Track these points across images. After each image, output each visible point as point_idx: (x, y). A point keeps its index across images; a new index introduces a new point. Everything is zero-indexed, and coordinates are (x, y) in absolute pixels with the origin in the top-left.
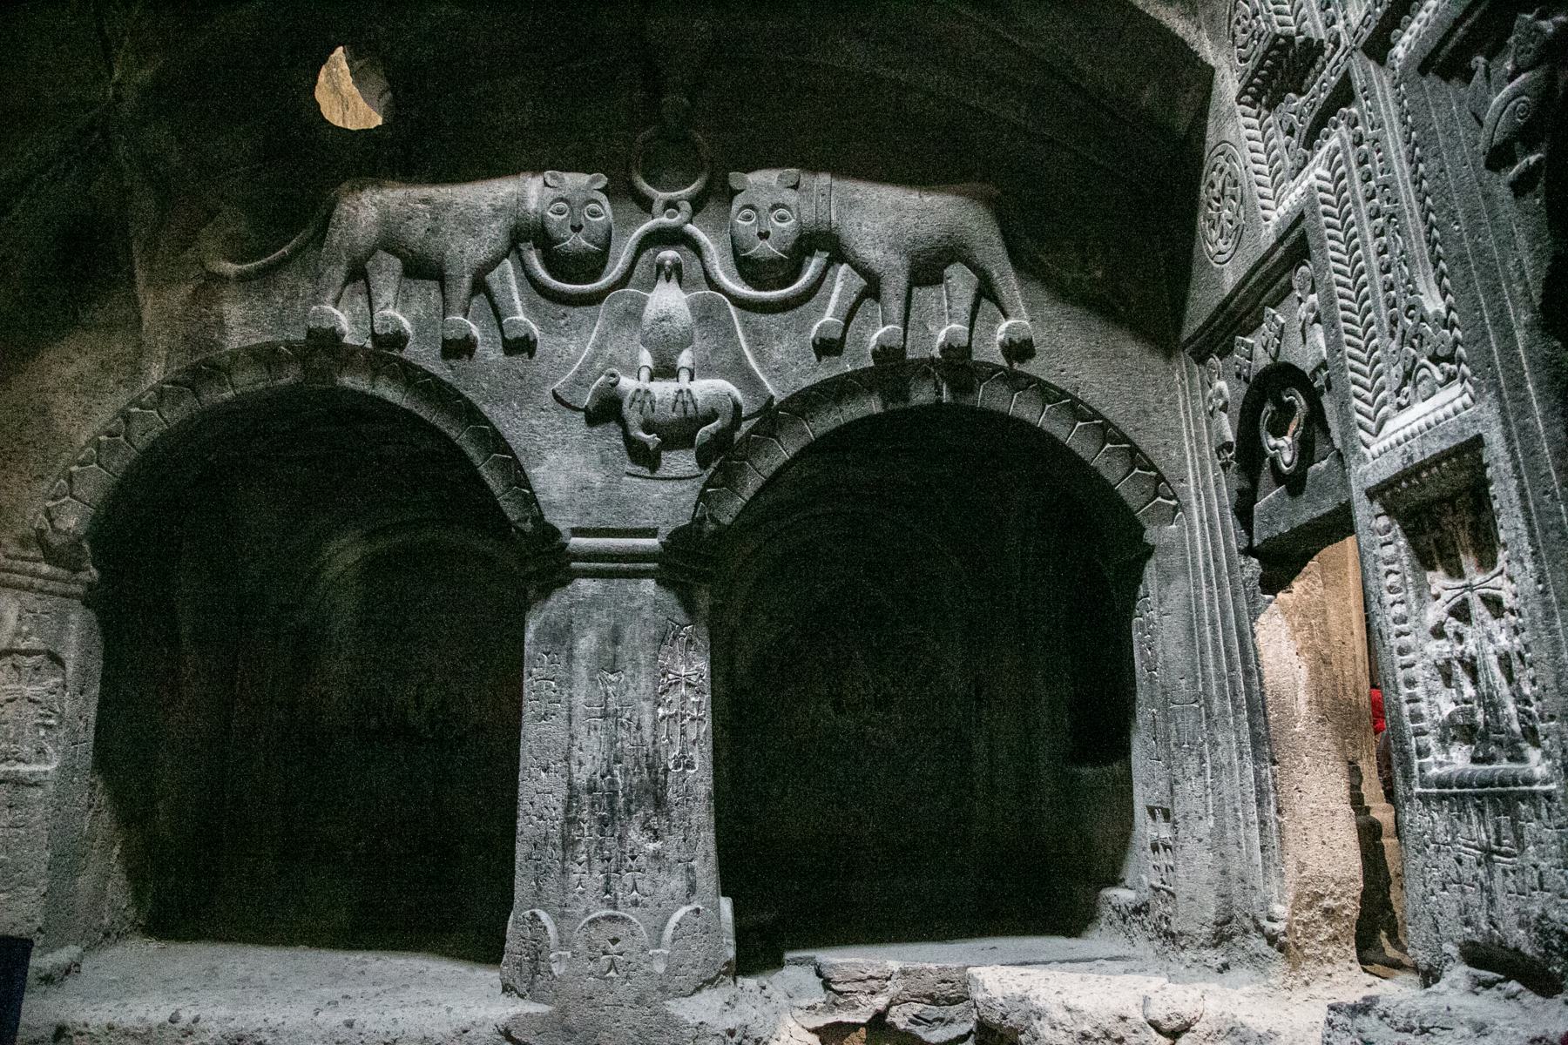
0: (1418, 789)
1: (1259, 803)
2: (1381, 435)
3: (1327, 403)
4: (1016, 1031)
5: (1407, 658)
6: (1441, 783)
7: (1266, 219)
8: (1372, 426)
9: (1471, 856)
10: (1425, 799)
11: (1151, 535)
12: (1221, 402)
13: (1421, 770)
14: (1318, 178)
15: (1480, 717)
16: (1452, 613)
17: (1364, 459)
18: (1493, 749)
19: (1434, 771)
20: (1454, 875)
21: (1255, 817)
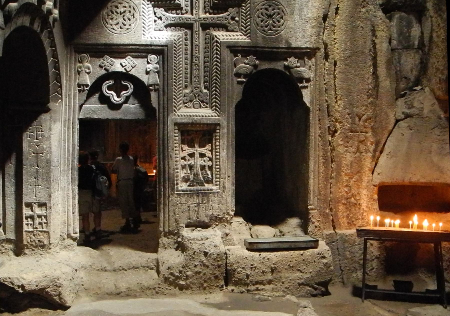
0: (176, 192)
1: (74, 198)
2: (180, 111)
3: (153, 95)
4: (43, 289)
5: (177, 163)
6: (183, 191)
7: (144, 35)
8: (178, 108)
9: (192, 205)
10: (179, 195)
11: (51, 105)
12: (88, 71)
13: (177, 188)
14: (175, 40)
15: (192, 177)
16: (189, 155)
17: (175, 115)
18: (195, 184)
19: (180, 188)
20: (187, 210)
21: (71, 203)
